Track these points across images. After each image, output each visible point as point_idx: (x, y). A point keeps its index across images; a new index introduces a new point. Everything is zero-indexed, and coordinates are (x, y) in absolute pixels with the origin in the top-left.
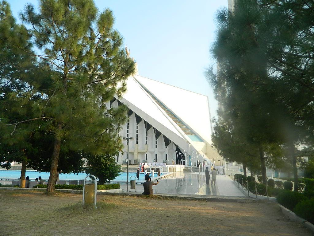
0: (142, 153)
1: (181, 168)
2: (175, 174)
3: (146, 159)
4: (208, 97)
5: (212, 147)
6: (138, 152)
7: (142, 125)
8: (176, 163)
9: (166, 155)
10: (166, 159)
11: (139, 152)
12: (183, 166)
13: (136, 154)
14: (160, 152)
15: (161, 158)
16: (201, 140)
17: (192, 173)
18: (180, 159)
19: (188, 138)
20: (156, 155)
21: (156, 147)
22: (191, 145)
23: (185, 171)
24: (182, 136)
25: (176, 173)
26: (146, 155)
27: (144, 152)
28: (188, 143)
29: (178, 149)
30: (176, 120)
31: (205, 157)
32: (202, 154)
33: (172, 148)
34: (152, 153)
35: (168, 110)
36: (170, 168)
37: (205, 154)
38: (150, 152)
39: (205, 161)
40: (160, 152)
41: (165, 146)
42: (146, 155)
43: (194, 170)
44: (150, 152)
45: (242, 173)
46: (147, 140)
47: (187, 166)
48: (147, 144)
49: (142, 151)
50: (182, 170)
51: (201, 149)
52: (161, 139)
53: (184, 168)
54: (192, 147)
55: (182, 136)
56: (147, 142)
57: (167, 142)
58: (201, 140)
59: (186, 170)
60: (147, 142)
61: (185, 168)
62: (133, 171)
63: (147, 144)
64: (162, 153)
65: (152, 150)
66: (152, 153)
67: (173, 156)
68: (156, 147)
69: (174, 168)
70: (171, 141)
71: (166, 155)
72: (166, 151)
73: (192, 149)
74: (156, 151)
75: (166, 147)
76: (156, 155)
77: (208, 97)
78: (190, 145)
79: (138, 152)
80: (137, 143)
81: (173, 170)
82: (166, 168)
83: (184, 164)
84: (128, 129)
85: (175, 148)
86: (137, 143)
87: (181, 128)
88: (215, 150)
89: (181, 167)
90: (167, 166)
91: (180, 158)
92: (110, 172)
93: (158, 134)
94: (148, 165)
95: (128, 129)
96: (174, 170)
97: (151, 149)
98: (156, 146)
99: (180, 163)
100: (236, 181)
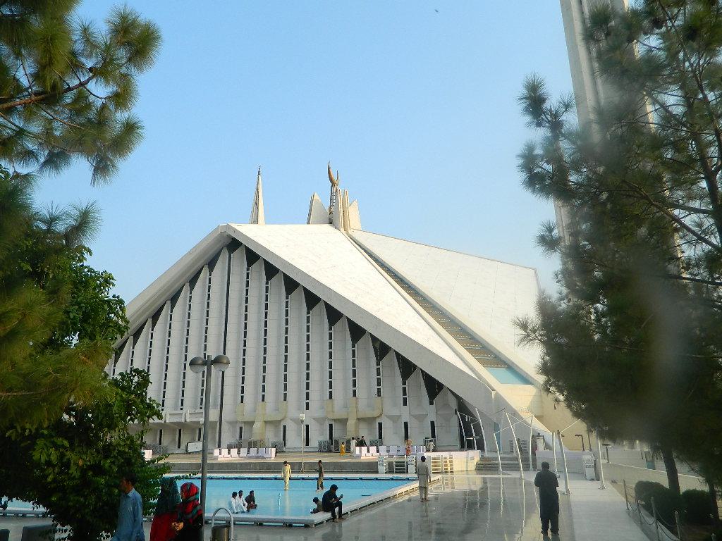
0: (369, 421)
1: (467, 462)
2: (452, 479)
3: (380, 436)
5: (548, 390)
6: (358, 419)
8: (459, 446)
9: (432, 423)
10: (433, 436)
11: (361, 416)
12: (475, 455)
13: (351, 423)
15: (419, 433)
16: (525, 380)
17: (501, 476)
18: (469, 438)
19: (488, 375)
20: (406, 424)
21: (405, 404)
22: (497, 393)
23: (481, 468)
24: (472, 369)
25: (455, 475)
26: (380, 425)
27: (374, 419)
28: (487, 389)
29: (463, 407)
30: (457, 329)
31: (538, 425)
32: (528, 417)
33: (446, 405)
34: (395, 419)
35: (409, 287)
36: (435, 460)
37: (539, 418)
38: (386, 416)
39: (536, 436)
41: (426, 399)
42: (380, 425)
44: (386, 416)
45: (660, 476)
47: (487, 454)
48: (379, 395)
49: (369, 414)
50: (472, 466)
51: (527, 404)
52: (416, 379)
53: (477, 459)
54: (498, 397)
55: (472, 369)
56: (379, 391)
57: (434, 388)
59: (484, 467)
60: (379, 391)
61: (482, 458)
62: (333, 472)
63: (379, 395)
64: (420, 418)
65: (395, 412)
66: (395, 419)
67: (450, 430)
68: (405, 404)
70: (441, 386)
71: (432, 423)
72: (431, 413)
73: (501, 405)
75: (431, 403)
76: (406, 424)
77: (535, 270)
78: (493, 393)
79: (358, 419)
80: (355, 395)
81: (446, 462)
83: (481, 447)
84: (331, 357)
85: (453, 404)
86: (355, 395)
87: (470, 350)
88: (557, 400)
89: (467, 458)
91: (469, 433)
92: (99, 498)
93: (407, 368)
94: (378, 451)
95: (331, 357)
96: (449, 468)
98: (405, 400)
99: (466, 445)
100: (643, 512)
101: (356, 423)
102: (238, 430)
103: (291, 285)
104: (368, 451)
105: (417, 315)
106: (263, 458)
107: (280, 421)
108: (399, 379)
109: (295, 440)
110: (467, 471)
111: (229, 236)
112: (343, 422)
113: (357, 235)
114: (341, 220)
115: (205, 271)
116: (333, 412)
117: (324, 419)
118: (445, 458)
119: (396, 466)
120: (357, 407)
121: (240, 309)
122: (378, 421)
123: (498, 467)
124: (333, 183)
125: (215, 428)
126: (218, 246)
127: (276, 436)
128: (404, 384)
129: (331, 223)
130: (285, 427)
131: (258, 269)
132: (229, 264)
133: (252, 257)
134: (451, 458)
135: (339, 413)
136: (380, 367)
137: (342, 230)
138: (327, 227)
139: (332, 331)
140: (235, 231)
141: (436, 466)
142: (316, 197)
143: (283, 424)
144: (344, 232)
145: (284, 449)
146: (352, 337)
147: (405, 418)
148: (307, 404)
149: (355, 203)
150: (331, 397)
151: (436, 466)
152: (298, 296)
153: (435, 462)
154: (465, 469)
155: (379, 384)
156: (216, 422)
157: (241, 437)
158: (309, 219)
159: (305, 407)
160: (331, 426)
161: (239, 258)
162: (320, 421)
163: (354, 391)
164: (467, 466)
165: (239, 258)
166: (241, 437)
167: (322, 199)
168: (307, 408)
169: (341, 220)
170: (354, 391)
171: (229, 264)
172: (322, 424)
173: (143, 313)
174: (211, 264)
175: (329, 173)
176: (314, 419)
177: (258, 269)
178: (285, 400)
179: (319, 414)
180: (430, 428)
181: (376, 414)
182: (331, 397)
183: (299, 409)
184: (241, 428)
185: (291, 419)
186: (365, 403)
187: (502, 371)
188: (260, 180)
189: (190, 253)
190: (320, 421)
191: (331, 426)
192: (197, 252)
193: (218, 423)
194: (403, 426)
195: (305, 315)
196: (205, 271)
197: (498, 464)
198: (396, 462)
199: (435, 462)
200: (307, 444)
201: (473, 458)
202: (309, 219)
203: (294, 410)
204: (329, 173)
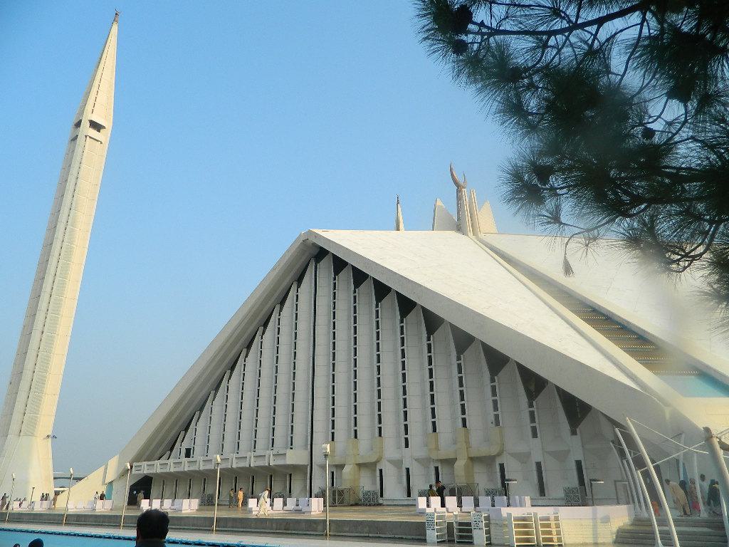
0: (487, 461)
1: (595, 527)
13: (460, 464)
14: (548, 453)
20: (539, 465)
21: (535, 435)
26: (502, 466)
34: (523, 458)
36: (524, 522)
38: (515, 455)
40: (548, 453)
43: (519, 539)
44: (515, 455)
46: (496, 408)
48: (497, 423)
49: (484, 450)
50: (607, 534)
56: (497, 417)
57: (576, 410)
60: (497, 417)
61: (638, 521)
63: (497, 423)
64: (561, 456)
65: (521, 448)
66: (523, 458)
69: (553, 523)
71: (579, 464)
72: (575, 447)
74: (536, 449)
75: (574, 433)
76: (539, 465)
79: (472, 459)
80: (464, 425)
82: (504, 524)
86: (464, 425)
89: (594, 519)
90: (505, 511)
93: (534, 384)
97: (518, 443)
101: (466, 466)
103: (382, 291)
104: (443, 505)
105: (551, 313)
106: (299, 511)
107: (374, 464)
108: (524, 399)
109: (394, 490)
111: (314, 245)
112: (450, 462)
113: (489, 239)
114: (469, 223)
115: (294, 287)
116: (437, 449)
117: (429, 460)
118: (548, 519)
119: (460, 531)
120: (467, 442)
121: (329, 328)
122: (498, 461)
123: (654, 539)
124: (459, 187)
126: (302, 260)
127: (374, 483)
128: (531, 405)
129: (459, 228)
130: (381, 471)
131: (346, 275)
132: (316, 276)
133: (339, 265)
134: (557, 519)
135: (445, 453)
137: (471, 234)
138: (453, 235)
139: (431, 342)
140: (317, 236)
141: (527, 533)
142: (439, 203)
143: (378, 467)
144: (473, 237)
145: (381, 502)
146: (457, 347)
147: (537, 456)
149: (487, 206)
150: (435, 430)
151: (527, 533)
152: (390, 303)
153: (525, 526)
154: (590, 540)
156: (306, 466)
157: (333, 485)
158: (433, 228)
159: (404, 444)
160: (437, 469)
161: (326, 266)
162: (424, 462)
163: (464, 421)
164: (595, 535)
165: (326, 266)
167: (445, 203)
168: (407, 446)
169: (469, 223)
170: (464, 421)
171: (316, 276)
173: (235, 342)
174: (299, 280)
175: (452, 175)
177: (346, 275)
178: (380, 435)
179: (421, 453)
180: (575, 473)
181: (494, 451)
182: (435, 430)
184: (333, 473)
185: (389, 461)
188: (400, 209)
189: (274, 269)
190: (424, 462)
191: (437, 469)
192: (282, 265)
194: (534, 467)
195: (398, 325)
196: (294, 287)
197: (653, 533)
198: (460, 524)
199: (525, 526)
200: (409, 495)
201: (606, 520)
202: (433, 228)
203: (391, 447)
204: (452, 175)
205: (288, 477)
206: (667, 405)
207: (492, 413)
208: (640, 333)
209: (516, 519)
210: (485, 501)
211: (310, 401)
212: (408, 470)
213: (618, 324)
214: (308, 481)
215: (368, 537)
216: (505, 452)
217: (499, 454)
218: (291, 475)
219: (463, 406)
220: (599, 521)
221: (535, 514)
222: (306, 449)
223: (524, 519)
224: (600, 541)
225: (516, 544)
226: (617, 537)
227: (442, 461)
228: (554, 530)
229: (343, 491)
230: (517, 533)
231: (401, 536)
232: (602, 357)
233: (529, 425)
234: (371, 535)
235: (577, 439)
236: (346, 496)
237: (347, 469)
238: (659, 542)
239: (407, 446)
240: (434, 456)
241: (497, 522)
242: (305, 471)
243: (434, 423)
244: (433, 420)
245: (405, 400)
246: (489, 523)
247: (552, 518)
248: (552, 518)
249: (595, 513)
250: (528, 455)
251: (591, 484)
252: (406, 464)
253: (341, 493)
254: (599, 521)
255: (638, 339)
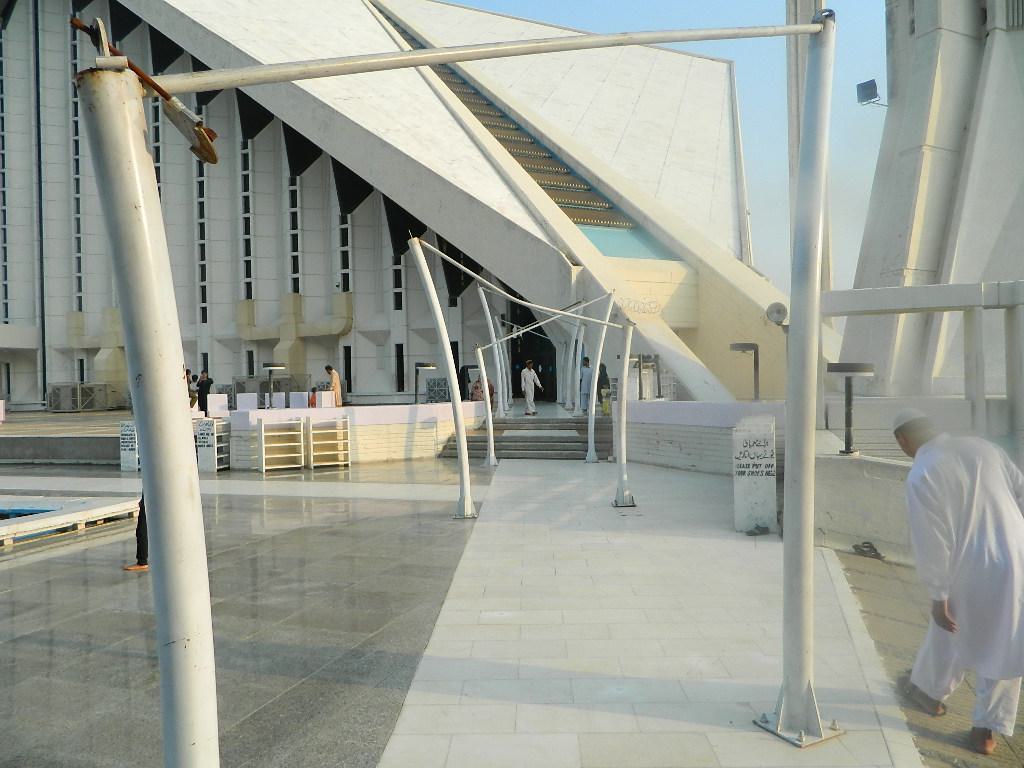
0: (327, 342)
4: (730, 63)
7: (319, 186)
11: (306, 332)
14: (417, 331)
16: (662, 247)
20: (399, 348)
21: (398, 306)
22: (585, 272)
26: (348, 350)
28: (562, 261)
34: (378, 338)
37: (686, 333)
40: (417, 331)
48: (346, 288)
51: (664, 301)
54: (587, 279)
56: (346, 277)
58: (662, 247)
60: (346, 277)
65: (378, 324)
66: (378, 338)
68: (398, 306)
69: (340, 432)
74: (397, 326)
76: (399, 348)
77: (730, 63)
78: (575, 271)
79: (305, 340)
80: (296, 289)
82: (250, 436)
86: (296, 289)
89: (411, 423)
90: (255, 415)
98: (398, 296)
102: (77, 365)
110: (408, 460)
112: (269, 344)
116: (251, 323)
122: (343, 343)
125: (35, 364)
136: (348, 226)
148: (204, 310)
150: (249, 295)
151: (294, 450)
154: (401, 455)
155: (345, 265)
156: (34, 351)
157: (82, 379)
160: (250, 354)
163: (296, 281)
164: (409, 448)
166: (82, 379)
168: (204, 320)
170: (296, 281)
172: (237, 353)
176: (219, 341)
179: (229, 332)
181: (336, 327)
182: (249, 295)
183: (193, 322)
184: (82, 361)
186: (319, 308)
187: (619, 235)
191: (250, 354)
193: (39, 353)
201: (431, 423)
205: (4, 371)
206: (577, 264)
207: (339, 271)
208: (572, 165)
209: (269, 428)
210: (217, 401)
211: (36, 244)
212: (205, 356)
213: (546, 149)
214: (40, 375)
215: (33, 464)
216: (353, 330)
217: (345, 332)
218: (8, 365)
219: (295, 259)
220: (418, 426)
221: (308, 419)
222: (35, 324)
223: (291, 428)
224: (415, 455)
225: (265, 468)
226: (445, 448)
227: (259, 343)
228: (341, 444)
229: (91, 389)
230: (268, 450)
231: (88, 461)
232: (507, 192)
233: (390, 290)
234: (36, 461)
235: (457, 310)
236: (98, 396)
237: (101, 357)
238: (492, 454)
239: (204, 320)
240: (247, 335)
241: (242, 434)
242: (32, 358)
243: (249, 285)
244: (248, 280)
245: (248, 263)
246: (229, 437)
247: (340, 423)
248: (340, 423)
249: (413, 414)
250: (387, 334)
251: (417, 371)
252: (203, 348)
253: (88, 392)
254: (418, 426)
255: (568, 173)
